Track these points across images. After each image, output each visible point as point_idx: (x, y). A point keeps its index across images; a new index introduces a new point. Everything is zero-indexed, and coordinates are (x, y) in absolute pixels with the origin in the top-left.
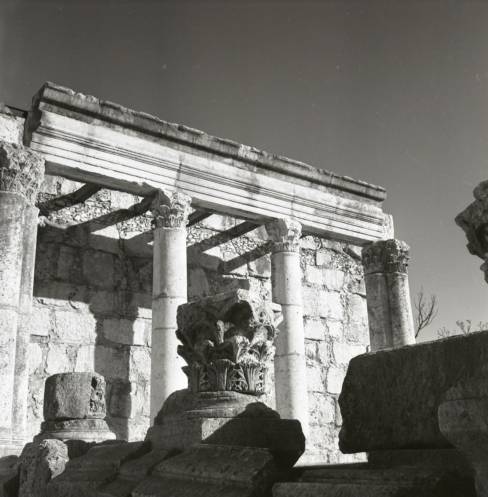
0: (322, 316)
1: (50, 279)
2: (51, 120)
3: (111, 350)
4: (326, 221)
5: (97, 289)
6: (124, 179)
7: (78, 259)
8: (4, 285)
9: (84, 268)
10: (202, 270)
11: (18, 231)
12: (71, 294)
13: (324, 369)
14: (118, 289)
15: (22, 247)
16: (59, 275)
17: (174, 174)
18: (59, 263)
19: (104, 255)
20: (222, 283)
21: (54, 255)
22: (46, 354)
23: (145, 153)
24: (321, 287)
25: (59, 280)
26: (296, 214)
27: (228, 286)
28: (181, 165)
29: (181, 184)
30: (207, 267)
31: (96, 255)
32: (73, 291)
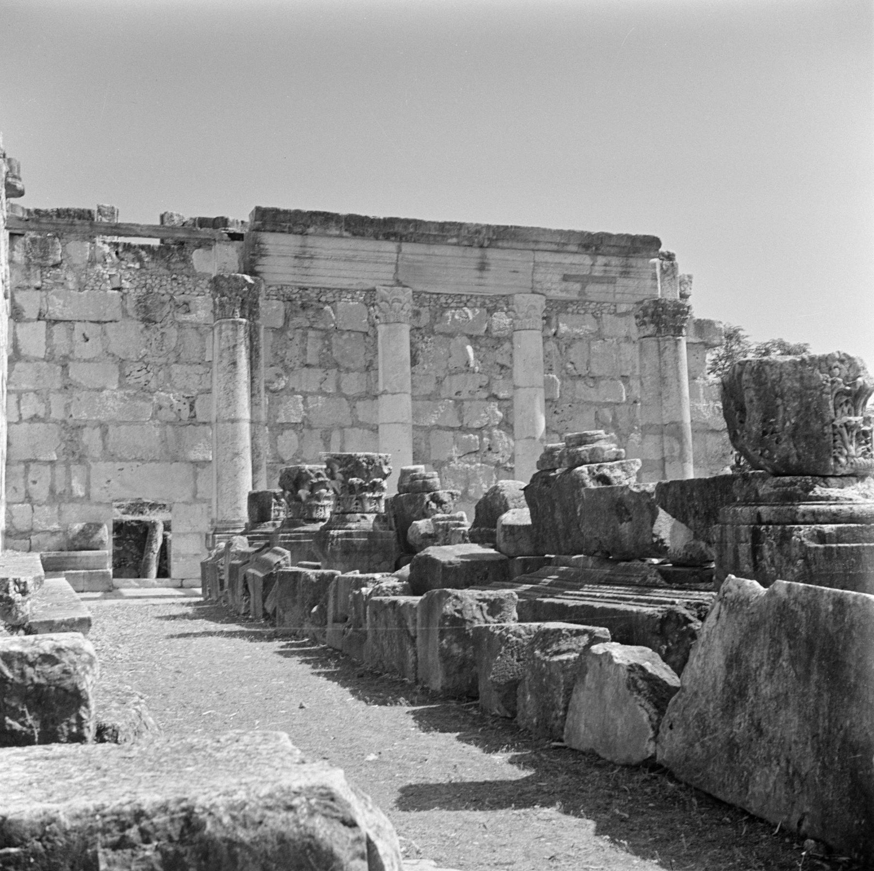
1: (300, 366)
2: (264, 241)
3: (366, 431)
5: (348, 370)
7: (327, 342)
9: (334, 350)
14: (370, 368)
16: (308, 361)
17: (393, 266)
18: (308, 348)
19: (353, 335)
21: (302, 341)
22: (301, 438)
24: (622, 339)
25: (307, 366)
31: (345, 336)
32: (324, 375)
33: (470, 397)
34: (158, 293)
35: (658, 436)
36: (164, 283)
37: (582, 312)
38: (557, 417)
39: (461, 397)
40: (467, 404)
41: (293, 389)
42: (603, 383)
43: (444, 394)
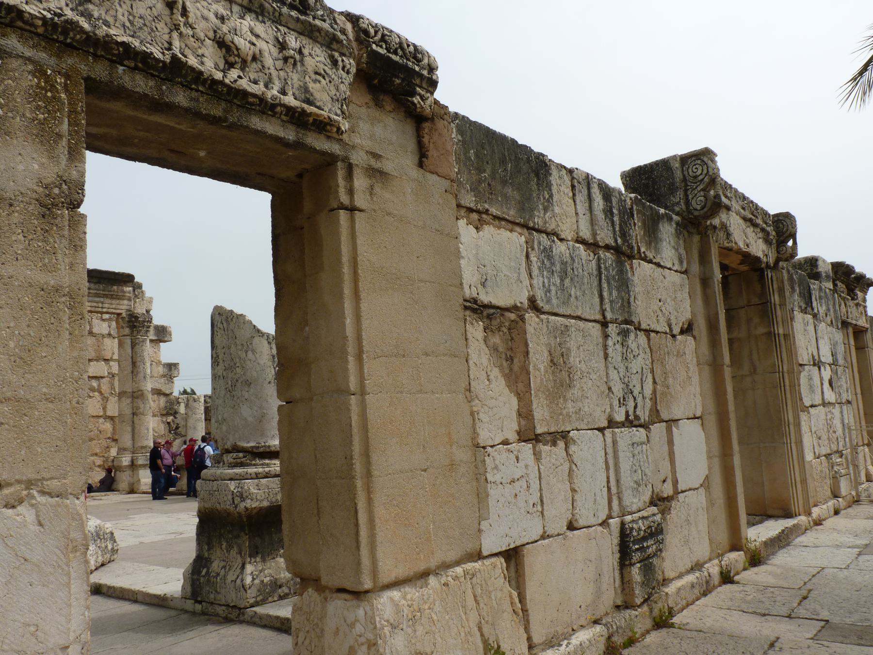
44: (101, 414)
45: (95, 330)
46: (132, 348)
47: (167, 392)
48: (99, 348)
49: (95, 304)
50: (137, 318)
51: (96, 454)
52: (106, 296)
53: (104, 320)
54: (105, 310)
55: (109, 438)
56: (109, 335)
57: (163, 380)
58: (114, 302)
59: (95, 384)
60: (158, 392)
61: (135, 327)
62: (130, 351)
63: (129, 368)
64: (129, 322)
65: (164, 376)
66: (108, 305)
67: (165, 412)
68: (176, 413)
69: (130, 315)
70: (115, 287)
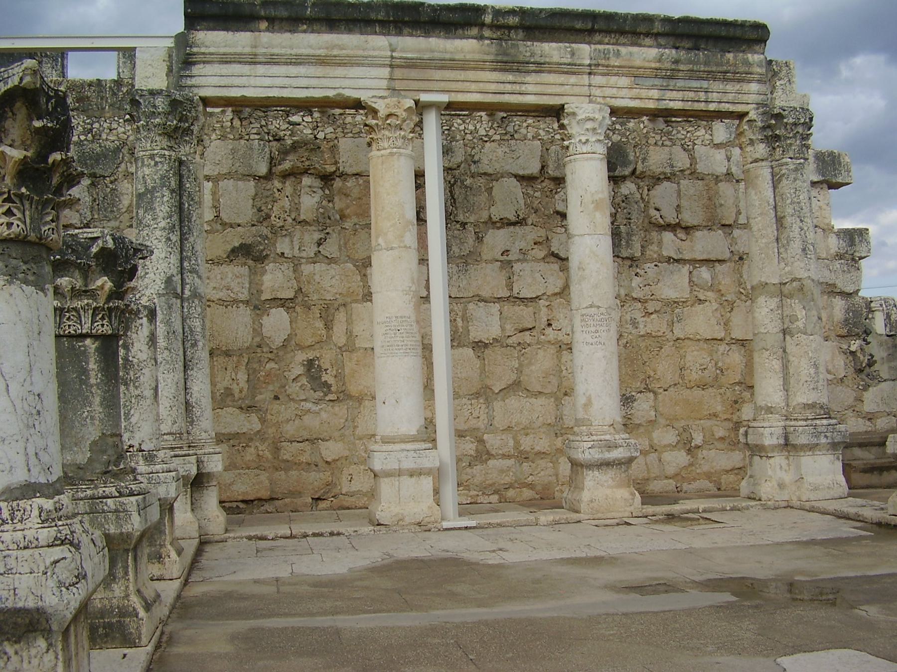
0: (723, 222)
4: (655, 93)
6: (309, 95)
7: (327, 192)
8: (155, 269)
10: (513, 179)
11: (165, 199)
12: (321, 239)
13: (725, 303)
15: (175, 217)
16: (302, 217)
17: (385, 72)
20: (548, 193)
23: (335, 52)
26: (597, 92)
27: (556, 196)
28: (392, 57)
29: (398, 85)
30: (521, 173)
32: (322, 236)
33: (521, 257)
34: (107, 140)
35: (777, 300)
36: (115, 126)
37: (668, 143)
38: (639, 279)
39: (510, 258)
40: (517, 267)
41: (283, 254)
42: (698, 234)
43: (487, 254)
44: (722, 335)
45: (700, 168)
46: (775, 188)
47: (850, 289)
48: (711, 204)
49: (691, 95)
50: (779, 117)
51: (715, 415)
52: (711, 76)
53: (717, 146)
54: (712, 107)
55: (740, 383)
56: (729, 174)
57: (837, 265)
58: (729, 87)
59: (704, 273)
60: (831, 290)
61: (777, 138)
62: (769, 193)
63: (772, 231)
64: (764, 128)
65: (840, 256)
66: (720, 95)
67: (844, 332)
68: (867, 332)
69: (764, 113)
70: (730, 56)
